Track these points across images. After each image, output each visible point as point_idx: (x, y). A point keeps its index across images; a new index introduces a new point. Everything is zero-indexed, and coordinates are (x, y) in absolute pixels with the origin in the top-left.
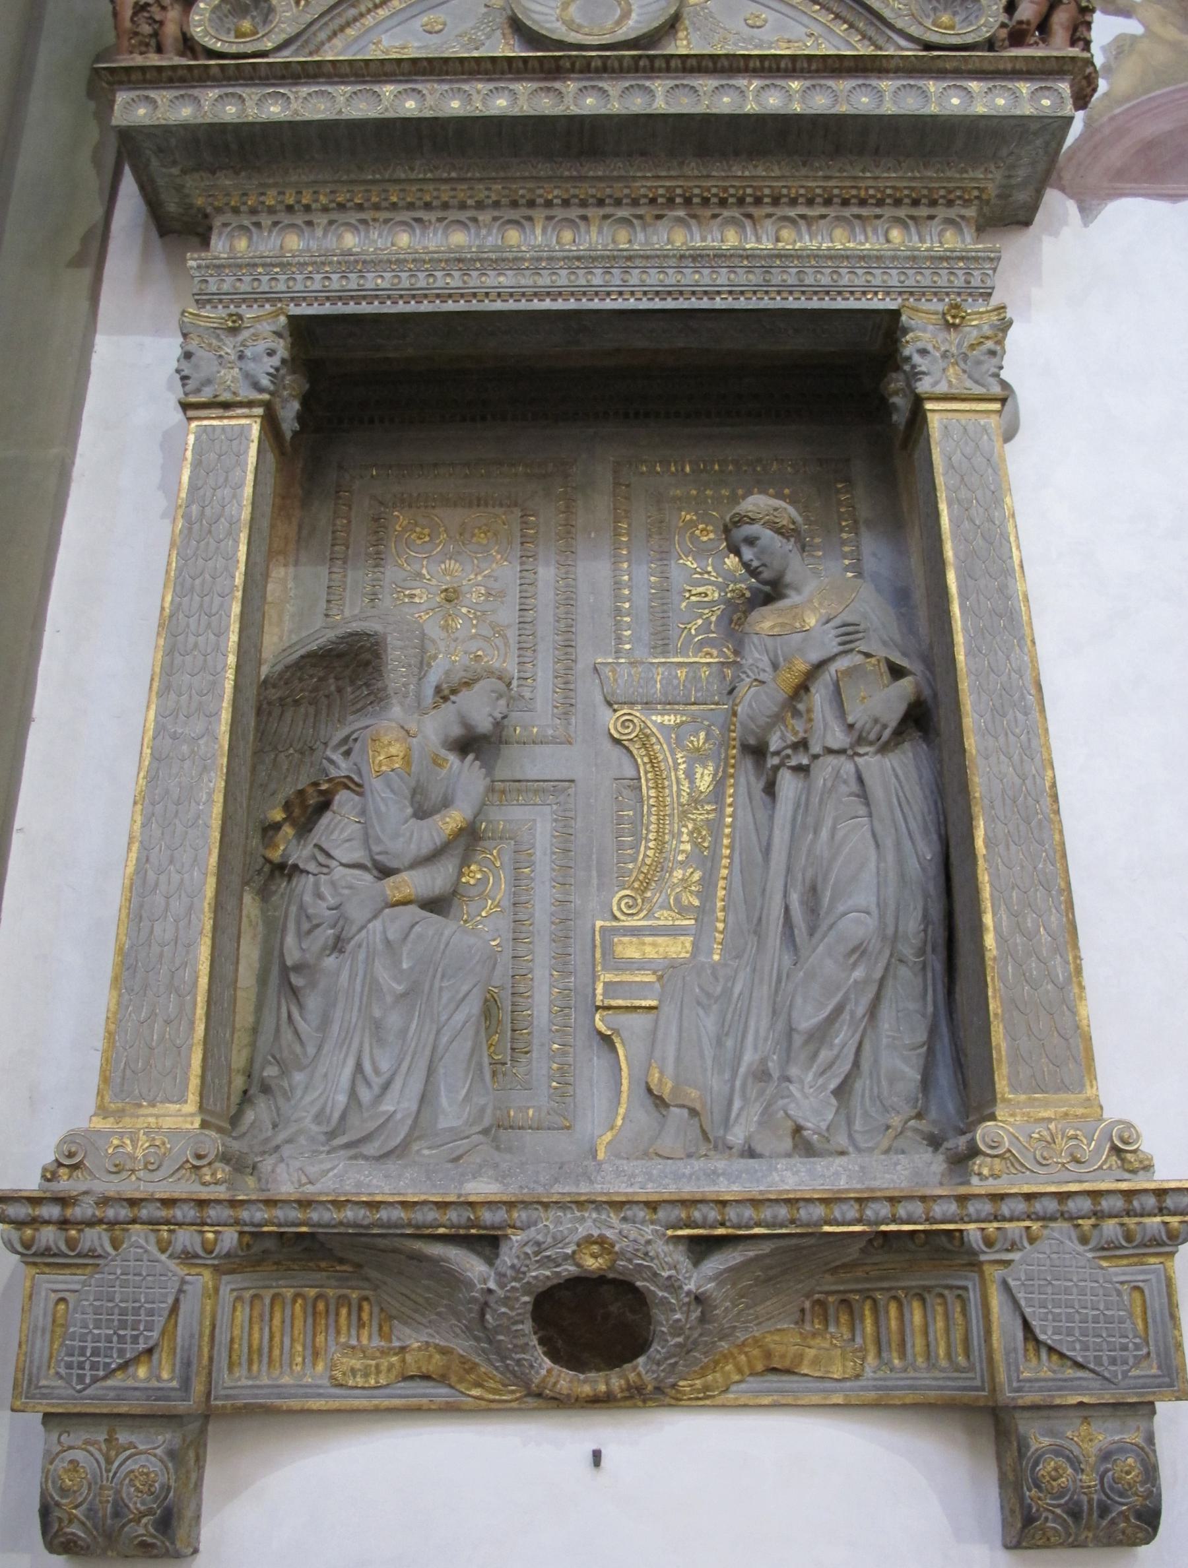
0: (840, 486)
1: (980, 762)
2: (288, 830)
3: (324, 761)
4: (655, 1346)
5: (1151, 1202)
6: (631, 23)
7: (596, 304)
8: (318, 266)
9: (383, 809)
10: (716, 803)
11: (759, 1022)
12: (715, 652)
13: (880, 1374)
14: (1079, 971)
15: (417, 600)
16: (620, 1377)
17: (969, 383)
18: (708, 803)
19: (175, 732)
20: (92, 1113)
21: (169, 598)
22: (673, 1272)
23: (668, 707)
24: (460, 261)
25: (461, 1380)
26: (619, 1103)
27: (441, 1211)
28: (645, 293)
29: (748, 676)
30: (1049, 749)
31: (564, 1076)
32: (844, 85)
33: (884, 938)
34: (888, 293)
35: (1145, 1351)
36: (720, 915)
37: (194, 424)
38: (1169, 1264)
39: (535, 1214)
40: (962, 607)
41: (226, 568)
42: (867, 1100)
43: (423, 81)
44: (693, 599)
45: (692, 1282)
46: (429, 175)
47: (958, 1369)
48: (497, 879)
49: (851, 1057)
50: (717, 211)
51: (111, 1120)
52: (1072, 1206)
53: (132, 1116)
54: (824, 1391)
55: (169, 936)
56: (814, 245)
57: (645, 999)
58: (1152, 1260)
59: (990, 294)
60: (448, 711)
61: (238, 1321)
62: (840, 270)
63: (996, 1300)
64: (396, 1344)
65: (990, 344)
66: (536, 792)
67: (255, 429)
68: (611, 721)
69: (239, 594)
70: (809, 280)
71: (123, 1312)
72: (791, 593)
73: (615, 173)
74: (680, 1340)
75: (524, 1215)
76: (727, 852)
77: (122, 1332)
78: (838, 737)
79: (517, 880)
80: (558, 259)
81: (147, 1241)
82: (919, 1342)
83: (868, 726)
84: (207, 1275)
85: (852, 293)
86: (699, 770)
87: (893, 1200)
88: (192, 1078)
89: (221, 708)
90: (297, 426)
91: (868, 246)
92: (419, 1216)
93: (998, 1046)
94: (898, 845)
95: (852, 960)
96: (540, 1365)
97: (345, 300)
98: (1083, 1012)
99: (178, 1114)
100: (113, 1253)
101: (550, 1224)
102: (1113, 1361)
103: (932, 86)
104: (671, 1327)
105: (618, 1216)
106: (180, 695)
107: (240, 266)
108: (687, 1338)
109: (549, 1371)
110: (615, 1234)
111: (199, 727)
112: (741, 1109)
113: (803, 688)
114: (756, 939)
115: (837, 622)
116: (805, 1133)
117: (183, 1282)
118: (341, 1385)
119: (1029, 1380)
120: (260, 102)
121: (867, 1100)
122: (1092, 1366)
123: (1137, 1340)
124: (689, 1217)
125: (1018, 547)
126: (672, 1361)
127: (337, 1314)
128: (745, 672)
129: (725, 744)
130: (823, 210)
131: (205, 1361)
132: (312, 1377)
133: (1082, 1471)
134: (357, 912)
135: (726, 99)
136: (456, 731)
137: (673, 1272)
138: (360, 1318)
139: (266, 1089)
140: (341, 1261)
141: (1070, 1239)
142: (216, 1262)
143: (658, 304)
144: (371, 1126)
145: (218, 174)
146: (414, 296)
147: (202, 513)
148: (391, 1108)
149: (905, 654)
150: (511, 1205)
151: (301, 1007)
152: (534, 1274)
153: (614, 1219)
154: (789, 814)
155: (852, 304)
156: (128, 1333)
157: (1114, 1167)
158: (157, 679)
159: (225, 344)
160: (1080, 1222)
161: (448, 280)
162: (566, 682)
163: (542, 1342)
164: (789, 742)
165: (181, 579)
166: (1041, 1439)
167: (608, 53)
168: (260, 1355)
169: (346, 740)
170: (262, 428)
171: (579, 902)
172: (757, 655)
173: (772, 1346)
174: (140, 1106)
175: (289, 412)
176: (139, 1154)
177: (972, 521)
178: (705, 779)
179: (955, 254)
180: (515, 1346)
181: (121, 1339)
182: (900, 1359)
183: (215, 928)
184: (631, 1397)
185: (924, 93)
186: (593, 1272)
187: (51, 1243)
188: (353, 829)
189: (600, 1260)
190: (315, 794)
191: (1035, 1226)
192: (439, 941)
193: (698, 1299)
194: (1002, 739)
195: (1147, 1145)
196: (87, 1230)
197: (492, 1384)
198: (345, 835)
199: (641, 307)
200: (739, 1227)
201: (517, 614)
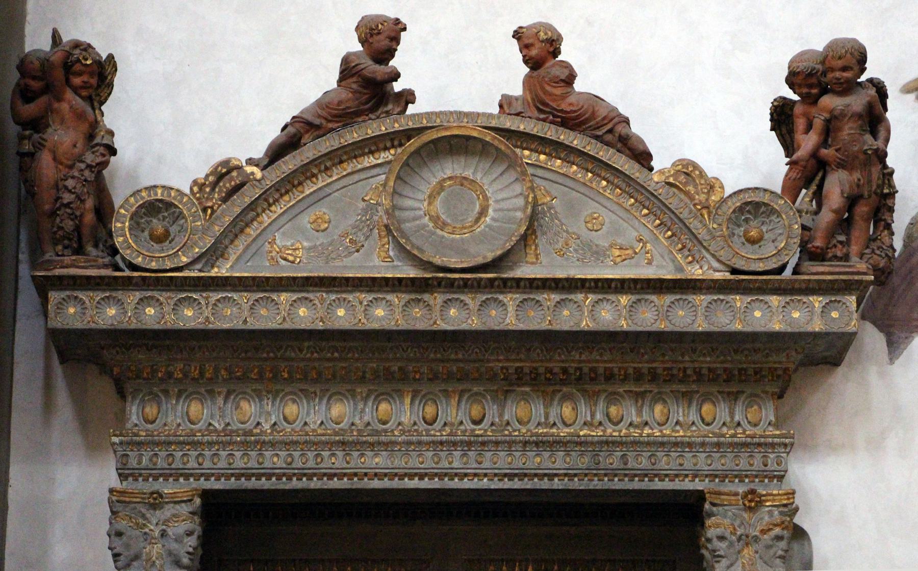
7: (456, 484)
28: (496, 475)
34: (695, 476)
56: (635, 432)
59: (783, 477)
65: (777, 531)
73: (473, 356)
85: (666, 475)
91: (681, 433)
97: (248, 477)
107: (158, 444)
143: (507, 484)
146: (305, 475)
155: (667, 485)
159: (149, 522)
167: (468, 276)
179: (756, 440)
199: (492, 487)
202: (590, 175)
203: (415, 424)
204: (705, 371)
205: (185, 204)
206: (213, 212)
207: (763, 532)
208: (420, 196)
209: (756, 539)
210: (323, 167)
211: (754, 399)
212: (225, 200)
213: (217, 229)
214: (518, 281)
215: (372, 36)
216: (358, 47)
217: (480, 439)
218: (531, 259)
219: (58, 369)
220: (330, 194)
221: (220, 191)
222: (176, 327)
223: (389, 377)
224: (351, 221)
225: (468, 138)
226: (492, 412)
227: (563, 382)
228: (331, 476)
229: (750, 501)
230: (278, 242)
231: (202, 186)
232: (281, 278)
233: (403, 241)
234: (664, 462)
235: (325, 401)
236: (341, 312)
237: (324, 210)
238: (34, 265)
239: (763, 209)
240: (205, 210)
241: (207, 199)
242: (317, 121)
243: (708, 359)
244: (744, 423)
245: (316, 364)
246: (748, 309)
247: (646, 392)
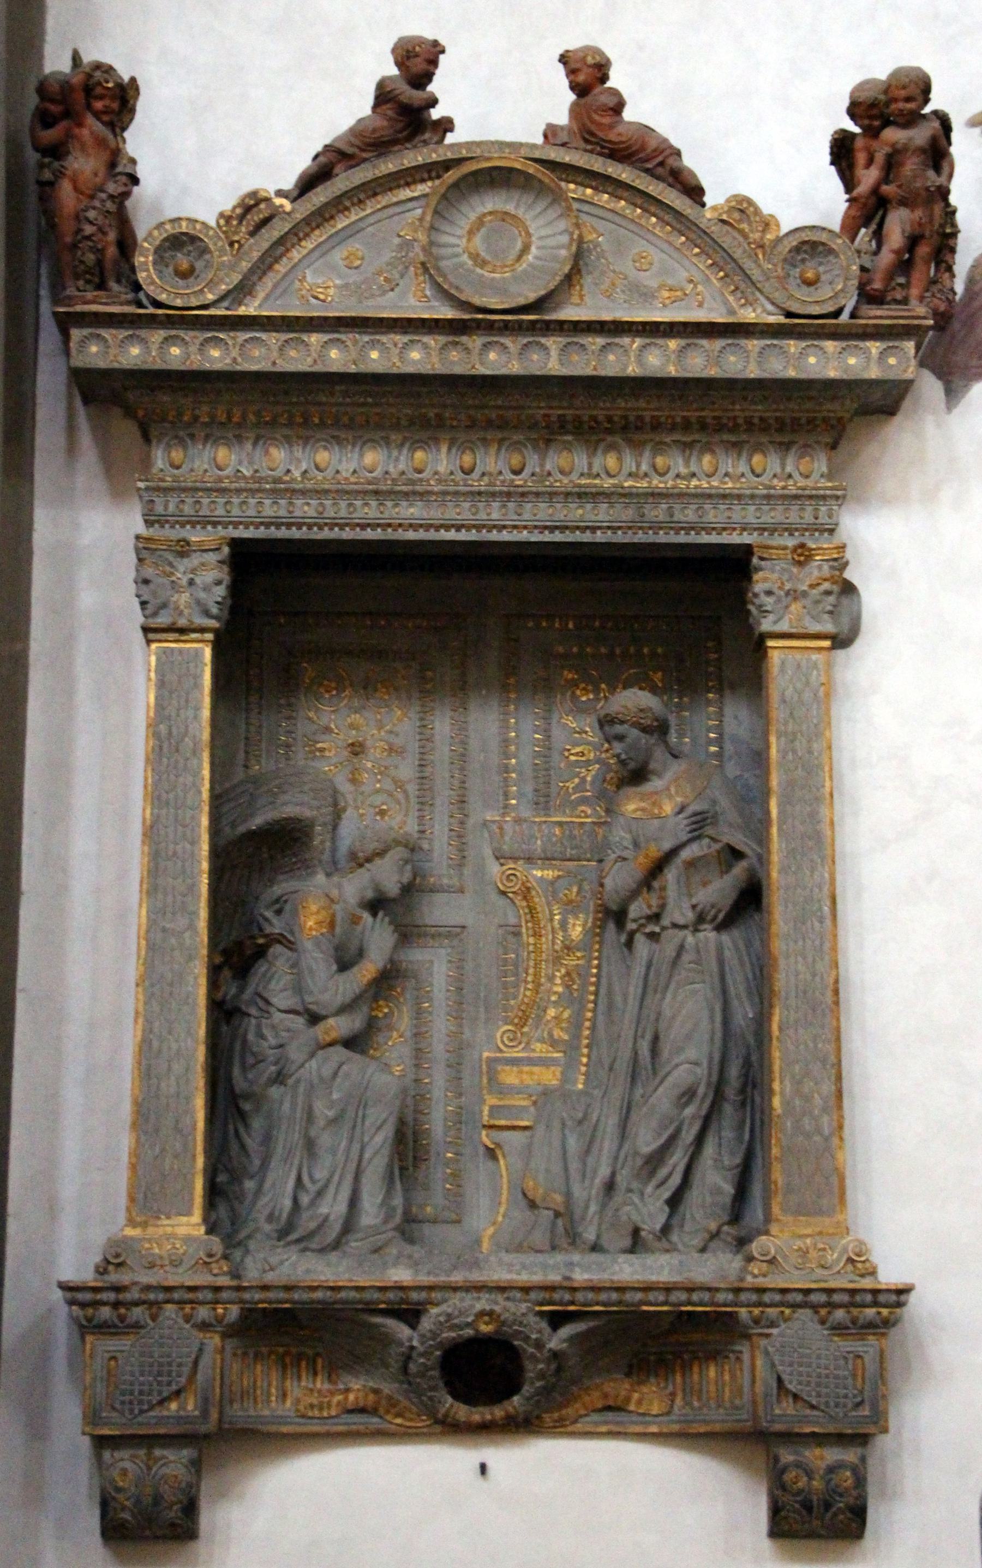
1: (782, 963)
5: (869, 1298)
6: (530, 257)
7: (494, 536)
14: (841, 1127)
25: (388, 1412)
28: (536, 527)
34: (744, 529)
35: (859, 1399)
37: (154, 646)
40: (780, 829)
41: (194, 784)
43: (345, 333)
47: (737, 1408)
52: (813, 1298)
55: (172, 1090)
56: (682, 484)
63: (759, 1363)
64: (342, 1387)
65: (826, 586)
67: (208, 652)
69: (206, 809)
70: (678, 516)
76: (591, 1006)
85: (714, 529)
87: (690, 1290)
89: (198, 909)
91: (730, 485)
93: (776, 1183)
97: (278, 526)
98: (840, 1156)
101: (456, 1302)
102: (837, 1405)
106: (165, 894)
107: (184, 490)
109: (452, 1406)
111: (182, 922)
118: (303, 1416)
119: (779, 1416)
122: (822, 1407)
125: (831, 778)
140: (302, 1328)
141: (812, 1321)
143: (547, 537)
146: (337, 525)
147: (170, 733)
153: (500, 1298)
155: (713, 539)
158: (145, 881)
163: (447, 1384)
170: (213, 650)
174: (159, 1218)
177: (794, 752)
179: (807, 492)
191: (787, 1311)
193: (555, 1355)
194: (800, 943)
197: (408, 1415)
200: (585, 1305)
202: (639, 211)
203: (452, 473)
204: (756, 421)
205: (210, 238)
206: (241, 246)
208: (459, 232)
209: (804, 594)
210: (355, 200)
211: (806, 449)
212: (252, 234)
213: (245, 265)
214: (561, 323)
215: (408, 58)
216: (394, 71)
217: (520, 490)
218: (575, 299)
220: (363, 229)
221: (248, 224)
222: (202, 368)
223: (425, 423)
224: (388, 255)
225: (511, 170)
226: (533, 461)
227: (609, 431)
228: (363, 527)
229: (799, 555)
230: (309, 279)
231: (228, 219)
232: (312, 318)
233: (440, 280)
234: (713, 515)
235: (357, 449)
236: (374, 355)
237: (357, 246)
238: (56, 301)
239: (821, 248)
240: (231, 244)
241: (236, 233)
242: (350, 150)
243: (760, 407)
244: (796, 475)
245: (349, 409)
246: (803, 354)
247: (694, 441)
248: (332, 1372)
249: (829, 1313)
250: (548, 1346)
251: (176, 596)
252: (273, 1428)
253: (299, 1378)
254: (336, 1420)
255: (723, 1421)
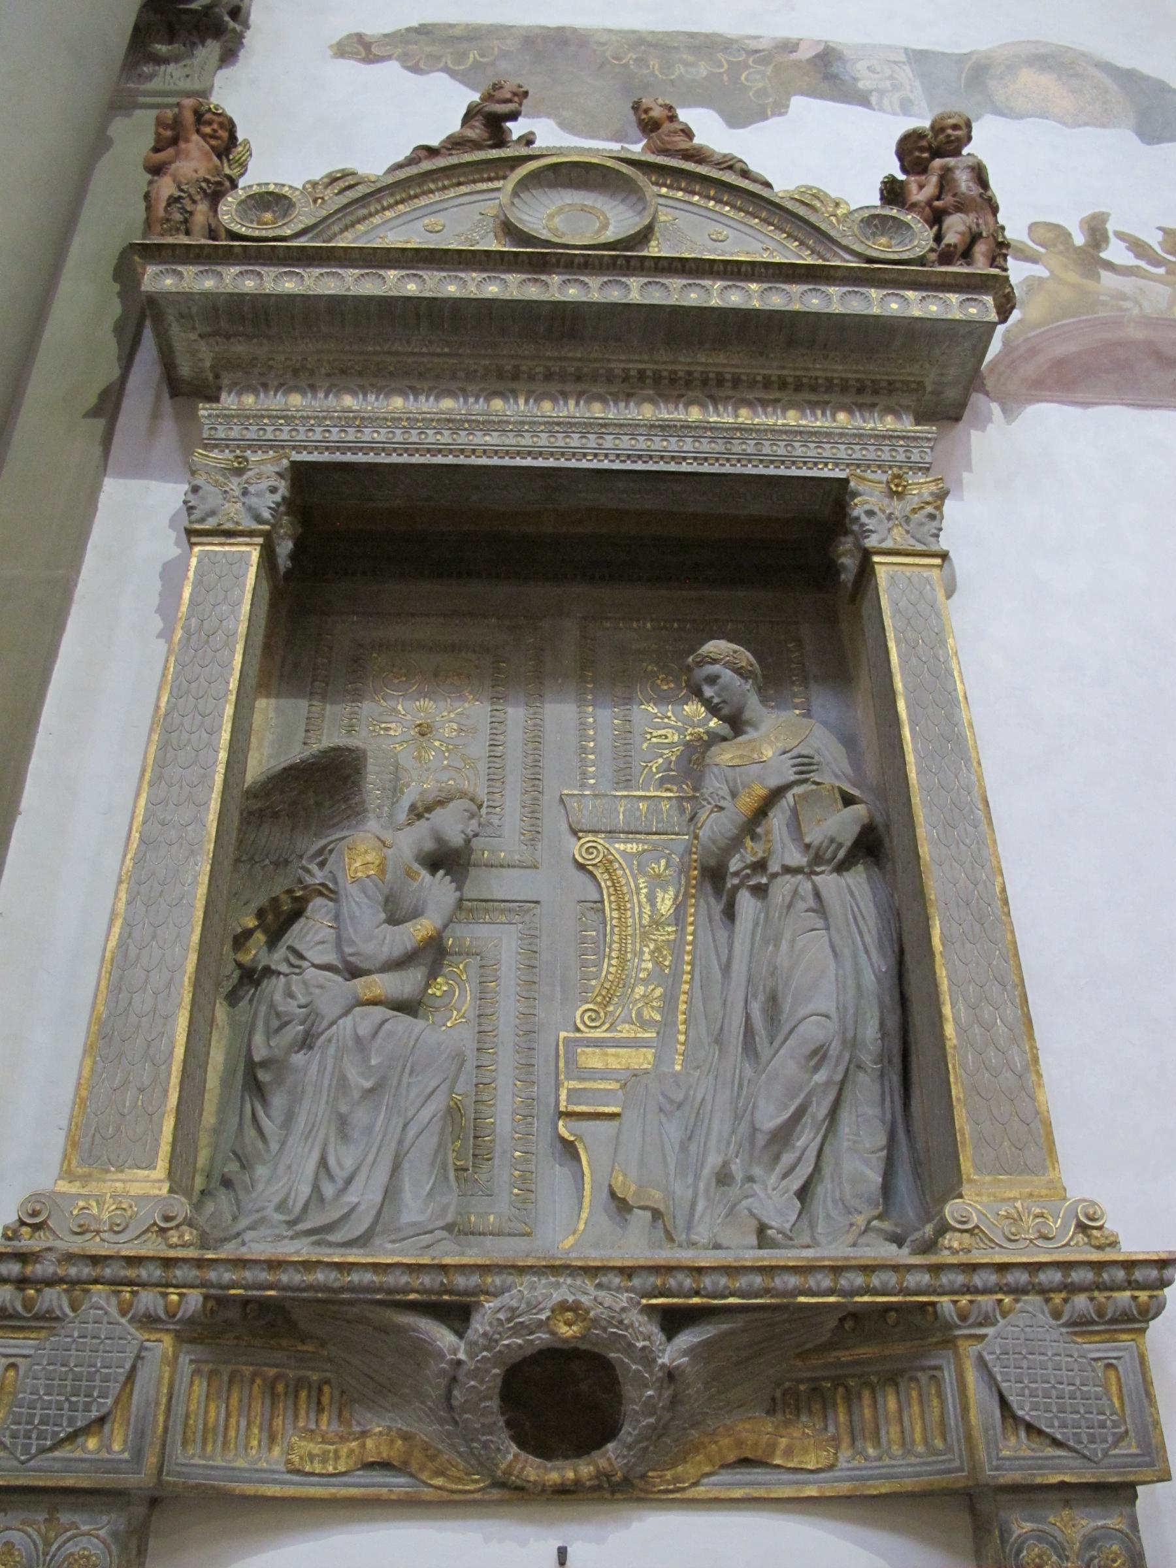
0: (790, 645)
2: (260, 937)
3: (300, 871)
4: (626, 1428)
5: (1120, 1274)
6: (608, 233)
7: (573, 464)
8: (320, 420)
9: (357, 914)
10: (677, 925)
11: (720, 1124)
12: (675, 788)
13: (855, 1463)
14: (1036, 1060)
15: (392, 733)
16: (588, 1464)
17: (913, 542)
18: (669, 925)
19: (164, 819)
20: (56, 1176)
21: (165, 699)
22: (647, 1343)
23: (630, 836)
24: (452, 423)
25: (422, 1468)
26: (581, 1208)
27: (414, 1275)
28: (618, 456)
29: (709, 803)
30: (997, 857)
31: (526, 1183)
32: (796, 289)
33: (844, 1042)
34: (837, 465)
36: (682, 1028)
37: (197, 549)
38: (1140, 1340)
39: (510, 1279)
40: (912, 730)
42: (829, 1203)
43: (423, 269)
44: (654, 740)
45: (666, 1356)
46: (424, 350)
48: (463, 991)
49: (813, 1160)
50: (683, 392)
51: (78, 1184)
52: (1043, 1277)
53: (99, 1180)
54: (797, 1483)
56: (771, 421)
57: (608, 1106)
58: (1124, 1337)
59: (928, 469)
60: (422, 826)
61: (195, 1395)
62: (795, 444)
63: (972, 1377)
65: (929, 509)
66: (503, 911)
67: (255, 555)
68: (576, 848)
69: (233, 698)
71: (77, 1378)
72: (749, 729)
73: (592, 356)
74: (652, 1420)
75: (498, 1280)
77: (74, 1399)
78: (796, 858)
79: (482, 995)
80: (540, 424)
81: (108, 1304)
82: (894, 1430)
83: (824, 845)
84: (168, 1341)
85: (805, 463)
86: (660, 894)
88: (162, 1145)
89: (210, 799)
90: (289, 564)
91: (818, 424)
92: (390, 1280)
94: (855, 956)
95: (812, 1063)
96: (507, 1448)
98: (1041, 1097)
99: (146, 1180)
100: (72, 1314)
101: (524, 1290)
103: (873, 293)
104: (645, 1404)
105: (592, 1282)
108: (659, 1420)
110: (590, 1300)
112: (706, 1209)
113: (762, 812)
114: (717, 1047)
115: (794, 753)
116: (770, 1232)
117: (142, 1348)
118: (297, 1472)
119: (1008, 1459)
120: (276, 279)
121: (829, 1203)
122: (1071, 1443)
123: (1115, 1417)
124: (664, 1284)
125: (962, 682)
126: (642, 1445)
127: (296, 1397)
128: (705, 799)
129: (684, 870)
130: (777, 395)
131: (160, 1430)
132: (268, 1462)
133: (1068, 1558)
134: (329, 1007)
135: (693, 295)
136: (429, 845)
137: (647, 1343)
138: (319, 1402)
139: (227, 1183)
141: (1043, 1312)
142: (178, 1327)
143: (629, 466)
144: (335, 1215)
145: (232, 340)
148: (355, 1200)
149: (855, 785)
150: (484, 1269)
151: (264, 1101)
152: (506, 1342)
153: (589, 1286)
154: (749, 933)
155: (805, 472)
156: (82, 1399)
157: (1081, 1243)
158: (149, 770)
160: (1052, 1295)
161: (439, 437)
162: (533, 810)
163: (509, 1424)
164: (748, 862)
165: (177, 683)
166: (1024, 1524)
168: (215, 1434)
169: (321, 852)
171: (542, 1015)
172: (717, 784)
173: (744, 1434)
174: (108, 1171)
175: (285, 548)
176: (105, 1216)
178: (666, 903)
180: (483, 1425)
181: (73, 1407)
182: (874, 1447)
183: (194, 1002)
184: (599, 1488)
185: (867, 298)
186: (566, 1341)
187: (8, 1305)
188: (328, 933)
189: (575, 1328)
190: (289, 901)
192: (409, 1037)
193: (671, 1375)
194: (953, 847)
195: (1111, 1224)
196: (47, 1290)
197: (453, 1472)
198: (318, 938)
199: (614, 467)
200: (715, 1297)
201: (488, 749)
207: (914, 511)
209: (907, 519)
219: (166, 396)
231: (314, 184)
245: (425, 360)
248: (346, 1402)
249: (1065, 1301)
250: (660, 1361)
251: (227, 505)
252: (249, 1489)
253: (296, 1416)
254: (346, 1479)
255: (918, 1475)
